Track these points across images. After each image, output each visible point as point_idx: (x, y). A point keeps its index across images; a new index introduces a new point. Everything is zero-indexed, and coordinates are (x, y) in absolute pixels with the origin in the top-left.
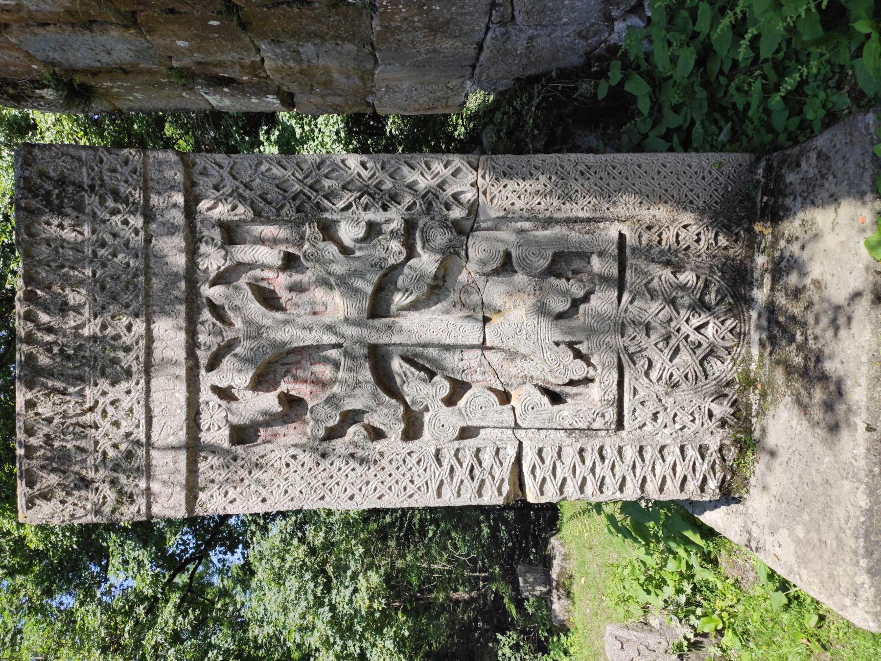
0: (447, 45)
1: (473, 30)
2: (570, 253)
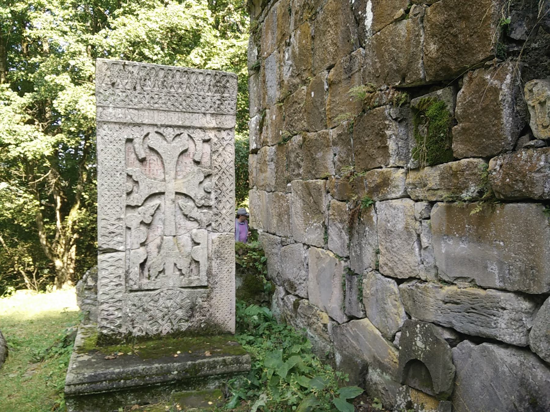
0: (275, 221)
1: (279, 231)
2: (199, 268)
